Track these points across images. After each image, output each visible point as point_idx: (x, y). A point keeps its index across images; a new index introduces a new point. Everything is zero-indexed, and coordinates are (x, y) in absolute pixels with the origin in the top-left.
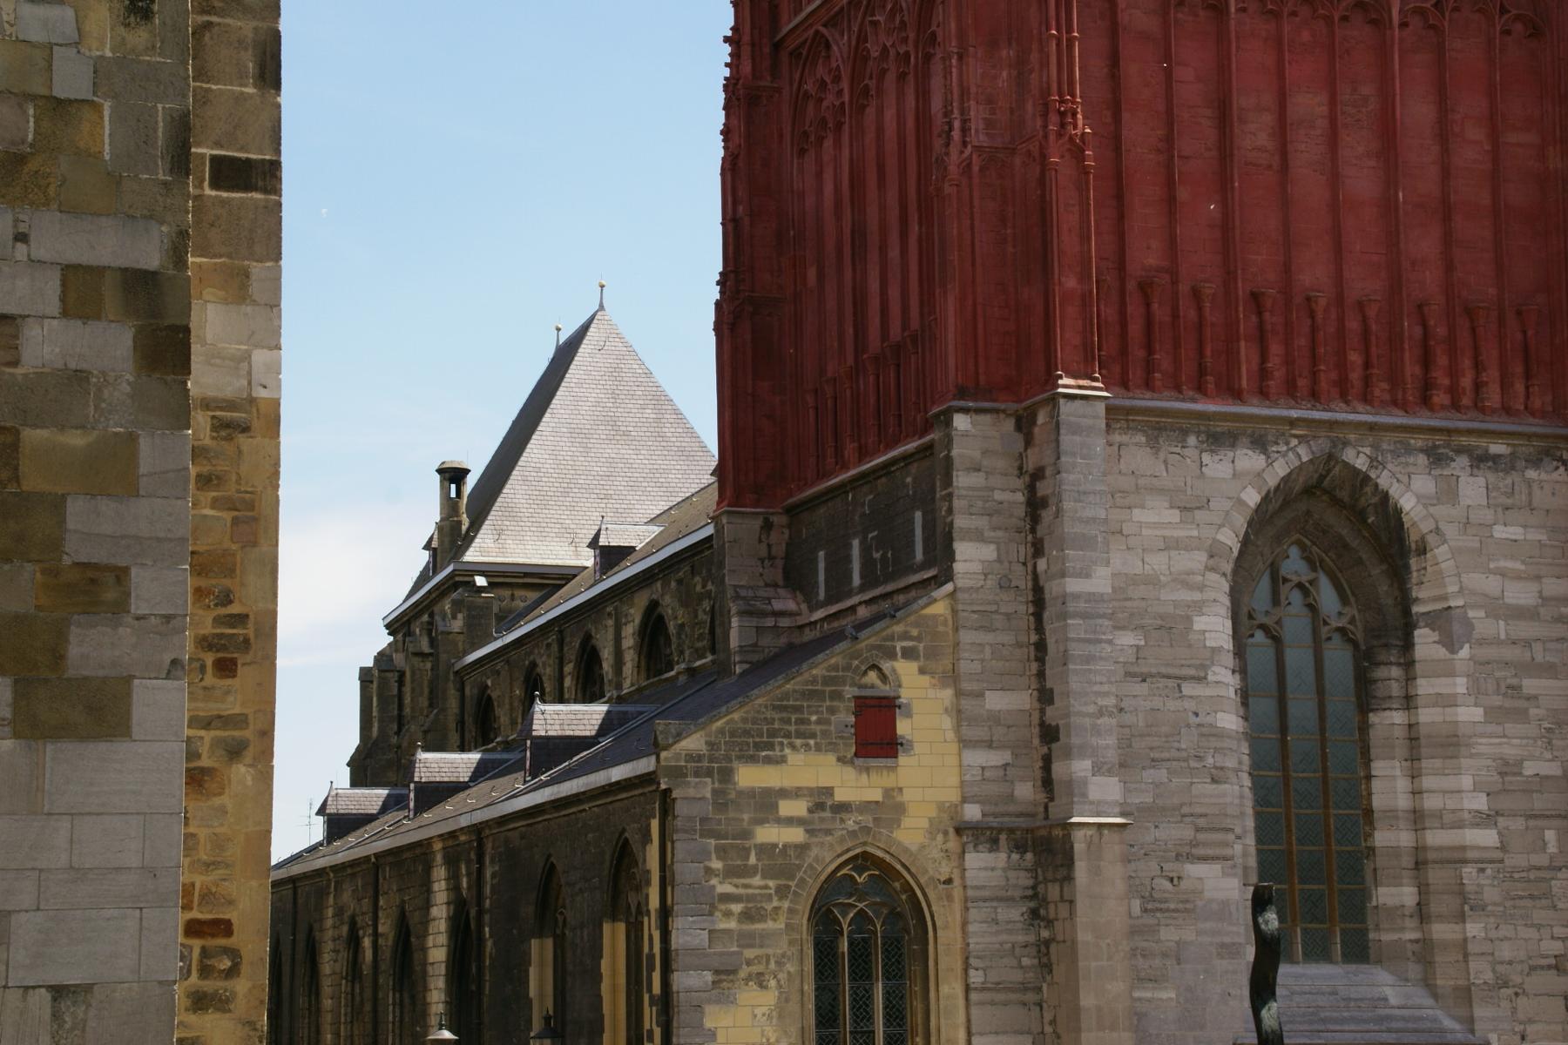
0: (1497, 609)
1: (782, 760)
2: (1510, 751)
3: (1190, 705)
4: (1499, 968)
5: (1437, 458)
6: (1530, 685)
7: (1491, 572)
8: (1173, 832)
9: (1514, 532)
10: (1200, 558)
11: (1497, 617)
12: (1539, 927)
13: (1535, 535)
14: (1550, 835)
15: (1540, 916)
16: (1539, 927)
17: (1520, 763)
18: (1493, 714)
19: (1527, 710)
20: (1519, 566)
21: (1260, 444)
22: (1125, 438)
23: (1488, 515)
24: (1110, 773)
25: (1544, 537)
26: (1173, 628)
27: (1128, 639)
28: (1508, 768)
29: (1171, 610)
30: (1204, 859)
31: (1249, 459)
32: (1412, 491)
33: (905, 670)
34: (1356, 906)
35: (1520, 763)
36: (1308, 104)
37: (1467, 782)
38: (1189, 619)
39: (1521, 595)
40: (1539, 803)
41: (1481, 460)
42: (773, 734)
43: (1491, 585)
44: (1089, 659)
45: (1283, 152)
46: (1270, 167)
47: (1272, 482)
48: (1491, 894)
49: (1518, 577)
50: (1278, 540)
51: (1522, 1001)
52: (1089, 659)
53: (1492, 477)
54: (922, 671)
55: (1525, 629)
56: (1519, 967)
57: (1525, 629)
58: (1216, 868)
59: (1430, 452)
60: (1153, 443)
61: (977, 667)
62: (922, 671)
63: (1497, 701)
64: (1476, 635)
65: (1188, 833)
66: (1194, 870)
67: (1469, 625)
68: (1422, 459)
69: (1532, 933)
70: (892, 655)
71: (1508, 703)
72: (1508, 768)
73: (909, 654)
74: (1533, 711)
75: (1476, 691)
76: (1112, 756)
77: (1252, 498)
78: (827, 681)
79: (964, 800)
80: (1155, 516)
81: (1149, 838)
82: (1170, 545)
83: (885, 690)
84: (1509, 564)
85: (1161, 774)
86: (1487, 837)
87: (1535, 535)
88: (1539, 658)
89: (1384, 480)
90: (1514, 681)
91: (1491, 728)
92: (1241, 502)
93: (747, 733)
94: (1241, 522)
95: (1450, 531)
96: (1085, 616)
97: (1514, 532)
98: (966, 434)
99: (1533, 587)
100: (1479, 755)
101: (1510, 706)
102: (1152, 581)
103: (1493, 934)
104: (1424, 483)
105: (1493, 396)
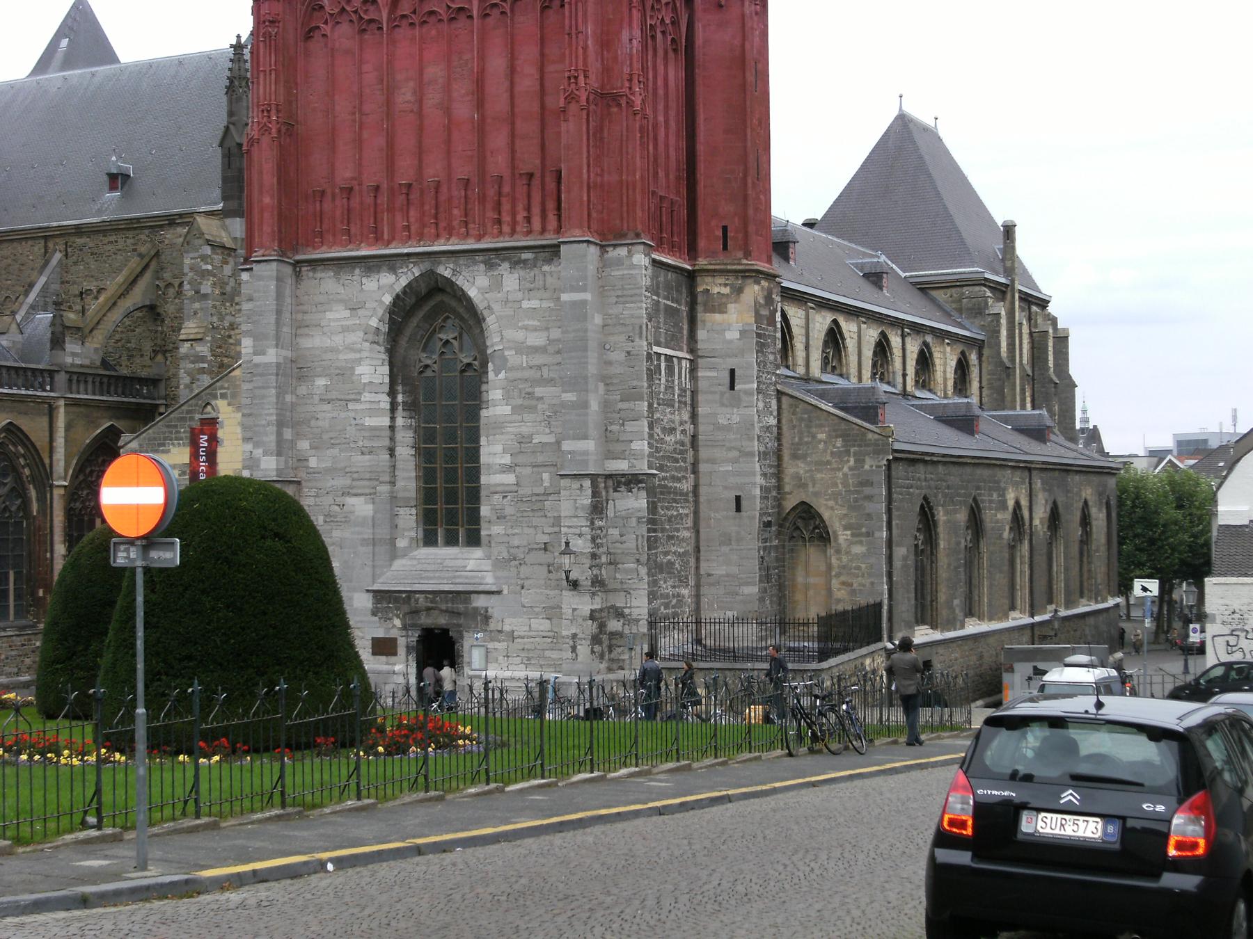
0: (521, 349)
1: (168, 451)
2: (525, 430)
3: (352, 414)
4: (512, 550)
5: (490, 266)
6: (539, 391)
7: (521, 328)
8: (340, 482)
9: (535, 303)
10: (361, 334)
11: (522, 354)
12: (535, 527)
13: (545, 304)
14: (546, 476)
15: (536, 521)
16: (535, 527)
17: (531, 436)
18: (516, 410)
19: (536, 407)
20: (536, 323)
21: (393, 269)
22: (323, 275)
23: (520, 295)
24: (271, 454)
25: (552, 305)
26: (345, 374)
27: (321, 382)
28: (523, 440)
29: (344, 364)
30: (356, 495)
31: (387, 278)
32: (475, 284)
33: (221, 404)
34: (474, 517)
35: (531, 436)
36: (435, 71)
37: (499, 448)
38: (353, 369)
39: (537, 339)
40: (541, 459)
41: (516, 264)
42: (165, 439)
43: (519, 335)
44: (263, 397)
45: (420, 101)
46: (412, 111)
47: (398, 288)
48: (509, 510)
49: (535, 329)
50: (430, 317)
51: (523, 568)
52: (263, 397)
53: (522, 273)
54: (229, 405)
55: (539, 359)
56: (522, 549)
57: (539, 359)
58: (362, 499)
59: (485, 263)
60: (337, 274)
61: (248, 401)
62: (229, 405)
63: (520, 402)
64: (509, 365)
65: (348, 482)
66: (350, 501)
67: (505, 359)
68: (482, 267)
69: (531, 531)
70: (215, 397)
71: (527, 403)
72: (523, 440)
73: (223, 396)
74: (540, 406)
75: (507, 398)
76: (273, 446)
77: (388, 299)
78: (189, 412)
79: (244, 468)
80: (337, 315)
81: (329, 485)
82: (345, 329)
83: (213, 415)
84: (531, 323)
85: (336, 451)
86: (510, 479)
87: (545, 304)
88: (545, 376)
89: (460, 281)
90: (530, 390)
91: (516, 417)
92: (381, 302)
93: (155, 439)
94: (380, 312)
95: (496, 307)
96: (261, 375)
97: (535, 303)
98: (247, 282)
99: (545, 334)
100: (508, 433)
101: (526, 403)
102: (334, 350)
103: (510, 531)
104: (482, 281)
105: (536, 223)
